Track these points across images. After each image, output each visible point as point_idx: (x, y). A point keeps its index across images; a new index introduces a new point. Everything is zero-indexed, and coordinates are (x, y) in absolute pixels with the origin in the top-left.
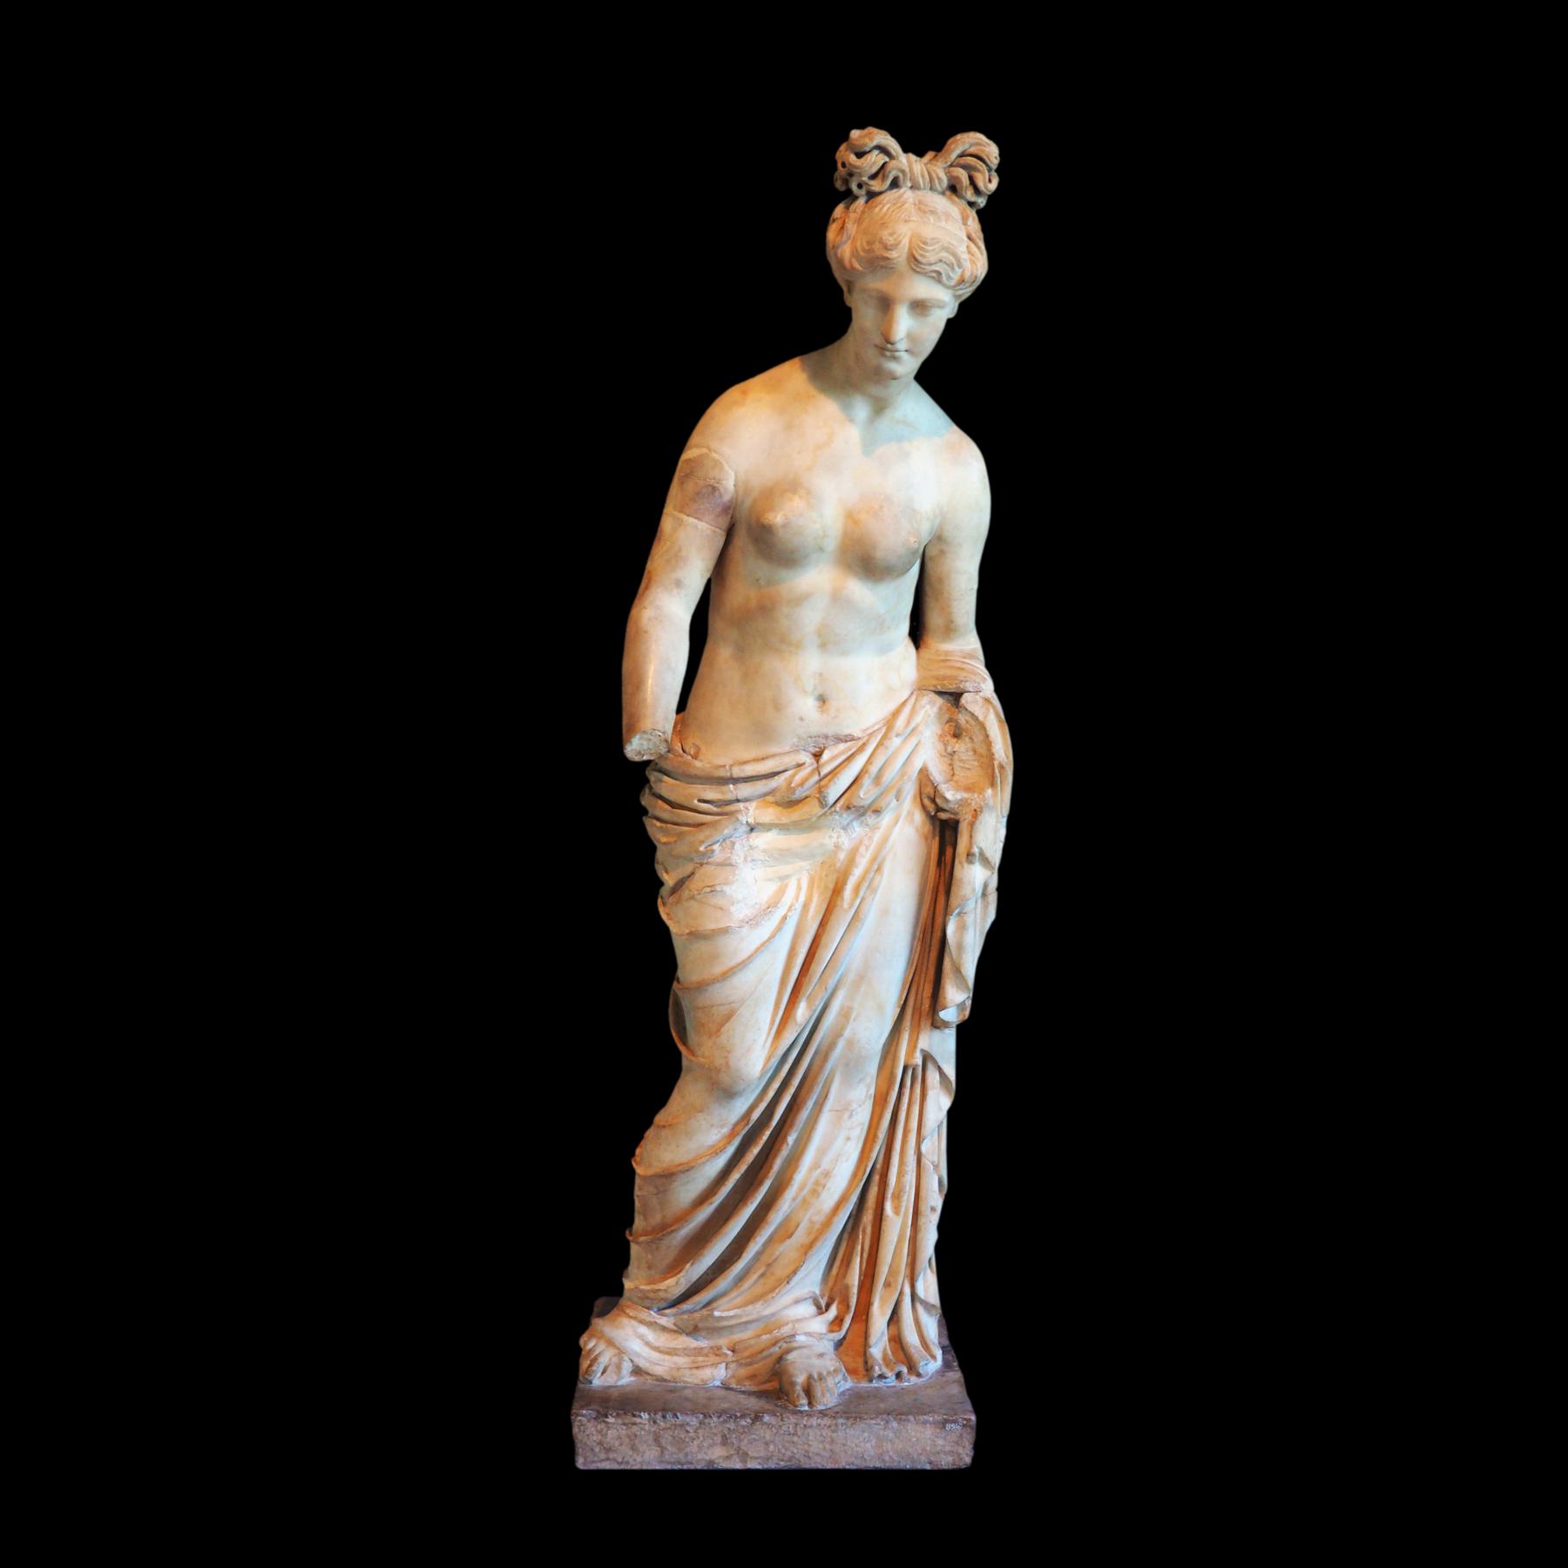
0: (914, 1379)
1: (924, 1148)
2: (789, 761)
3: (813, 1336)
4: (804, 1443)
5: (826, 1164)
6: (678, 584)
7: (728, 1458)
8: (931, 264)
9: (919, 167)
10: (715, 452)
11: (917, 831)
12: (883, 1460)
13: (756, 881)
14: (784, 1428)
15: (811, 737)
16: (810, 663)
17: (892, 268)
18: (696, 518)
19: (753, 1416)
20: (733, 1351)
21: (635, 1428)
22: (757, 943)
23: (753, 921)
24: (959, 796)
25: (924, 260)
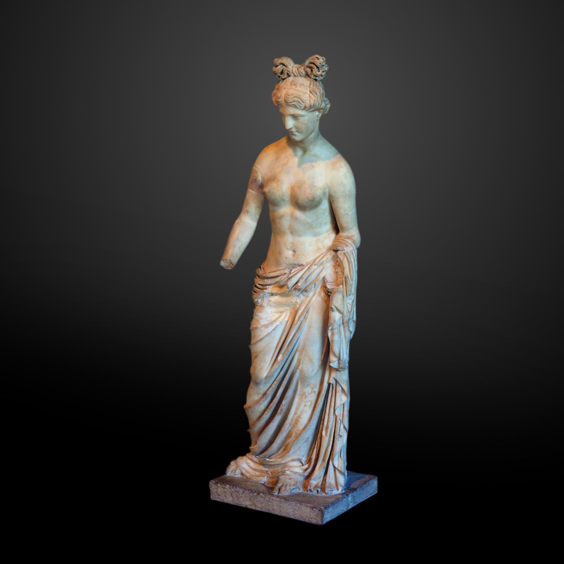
0: (324, 494)
1: (336, 413)
2: (282, 272)
3: (293, 473)
4: (272, 506)
5: (298, 412)
6: (247, 212)
7: (251, 505)
8: (291, 103)
9: (295, 69)
10: (257, 168)
11: (322, 298)
12: (295, 517)
13: (272, 312)
14: (266, 499)
15: (290, 264)
16: (289, 239)
17: (281, 105)
18: (252, 190)
19: (257, 493)
20: (272, 473)
21: (225, 490)
22: (266, 333)
23: (266, 326)
24: (332, 287)
25: (288, 101)
